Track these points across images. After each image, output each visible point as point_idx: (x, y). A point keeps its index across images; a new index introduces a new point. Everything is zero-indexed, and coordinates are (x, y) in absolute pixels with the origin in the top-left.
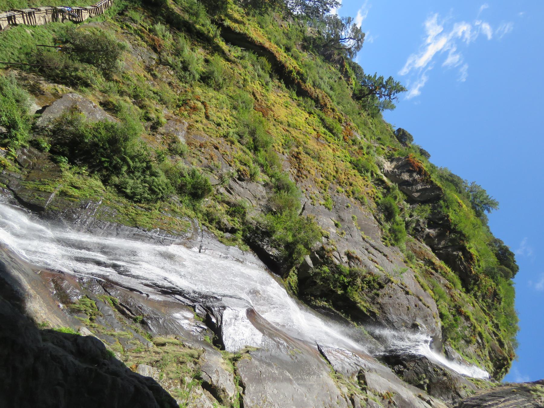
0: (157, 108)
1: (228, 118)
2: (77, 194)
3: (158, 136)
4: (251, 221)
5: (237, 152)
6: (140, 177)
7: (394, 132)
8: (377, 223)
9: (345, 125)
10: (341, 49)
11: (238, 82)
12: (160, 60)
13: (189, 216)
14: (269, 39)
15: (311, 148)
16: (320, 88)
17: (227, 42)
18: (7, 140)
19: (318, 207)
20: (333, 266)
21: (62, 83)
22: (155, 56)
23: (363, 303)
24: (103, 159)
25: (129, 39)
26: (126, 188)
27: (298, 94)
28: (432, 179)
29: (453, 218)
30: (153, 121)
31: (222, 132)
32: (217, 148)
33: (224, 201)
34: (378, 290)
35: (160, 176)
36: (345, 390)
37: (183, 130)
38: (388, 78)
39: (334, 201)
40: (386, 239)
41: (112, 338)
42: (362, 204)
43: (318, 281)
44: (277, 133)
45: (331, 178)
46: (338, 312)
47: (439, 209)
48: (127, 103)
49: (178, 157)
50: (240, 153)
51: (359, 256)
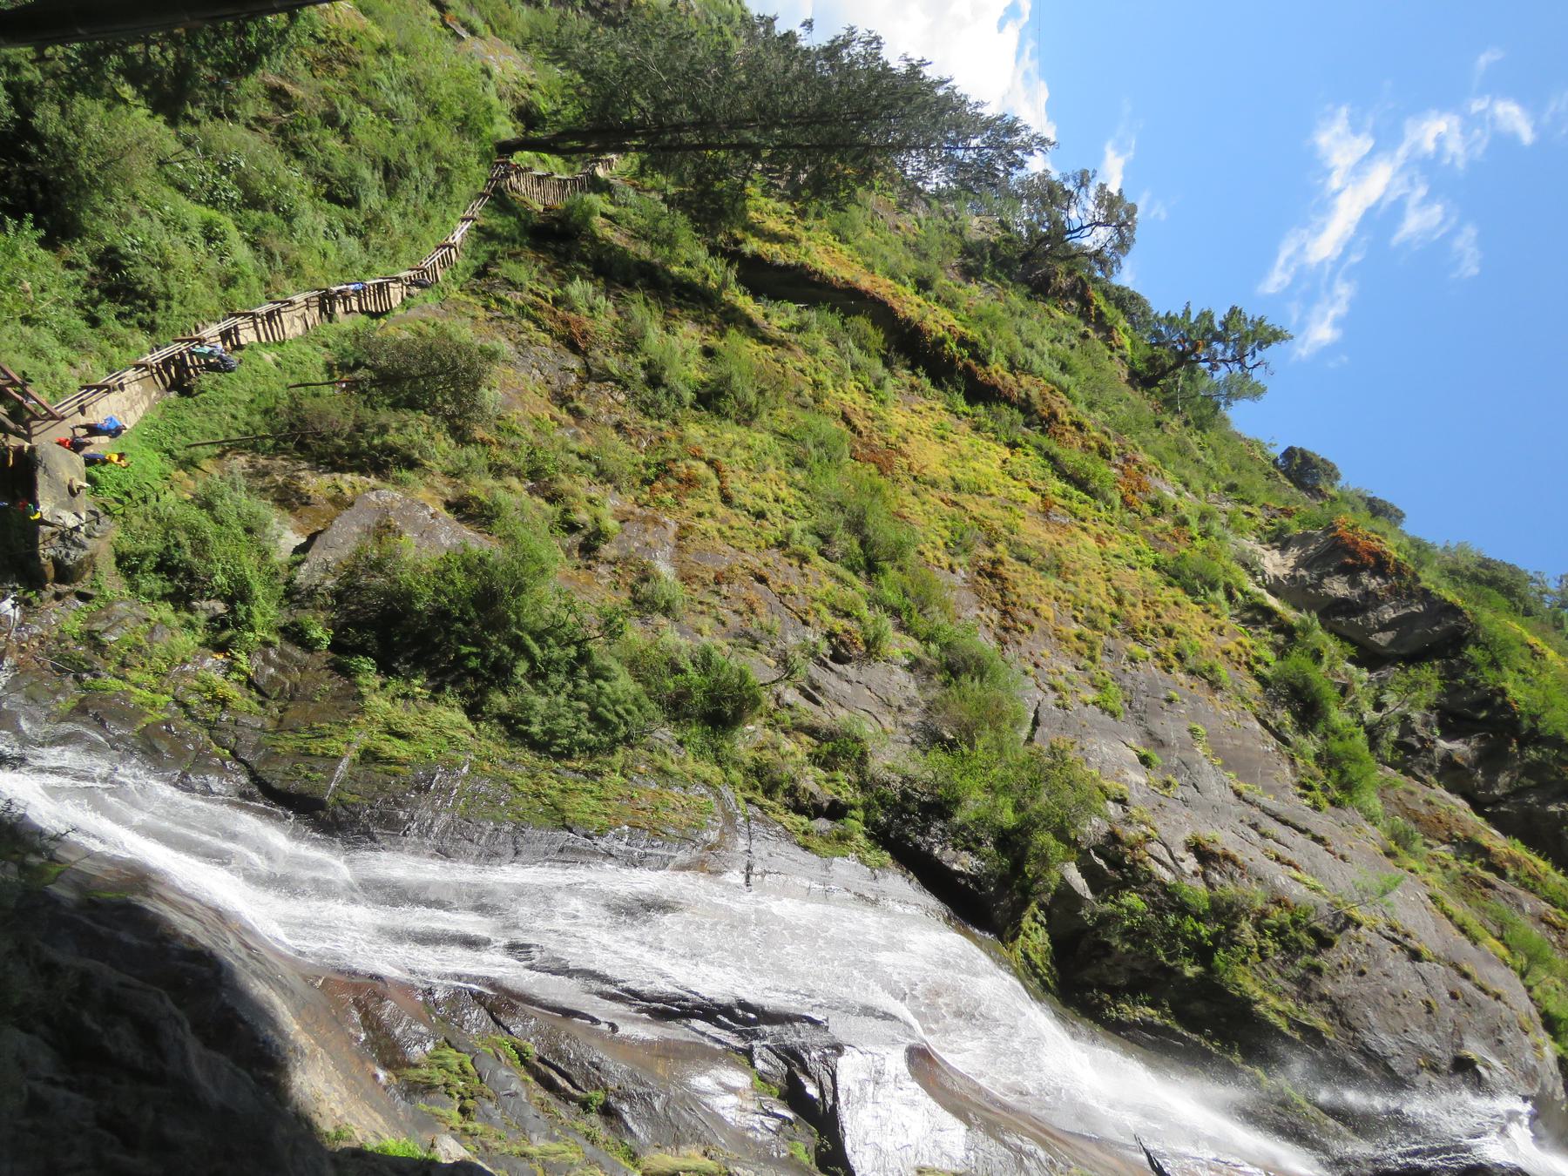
0: (593, 495)
1: (783, 494)
2: (404, 754)
3: (602, 570)
4: (884, 775)
5: (820, 583)
6: (563, 685)
7: (1275, 462)
8: (1272, 739)
9: (1120, 462)
10: (1074, 256)
11: (799, 394)
12: (588, 370)
13: (705, 782)
14: (870, 267)
15: (1032, 541)
16: (1031, 372)
17: (756, 297)
18: (228, 633)
19: (1078, 713)
20: (1156, 889)
21: (351, 470)
22: (574, 363)
23: (1272, 1001)
24: (465, 650)
25: (507, 333)
26: (528, 723)
27: (971, 399)
28: (1424, 584)
29: (1519, 696)
30: (585, 532)
31: (771, 533)
32: (762, 580)
33: (799, 728)
34: (1315, 954)
35: (616, 679)
37: (664, 543)
38: (1226, 311)
39: (1124, 688)
40: (1310, 788)
41: (526, 1165)
42: (1215, 686)
43: (1115, 942)
44: (926, 513)
45: (1106, 621)
46: (1195, 1037)
47: (1471, 675)
48: (514, 496)
49: (659, 619)
50: (830, 584)
51: (1232, 851)
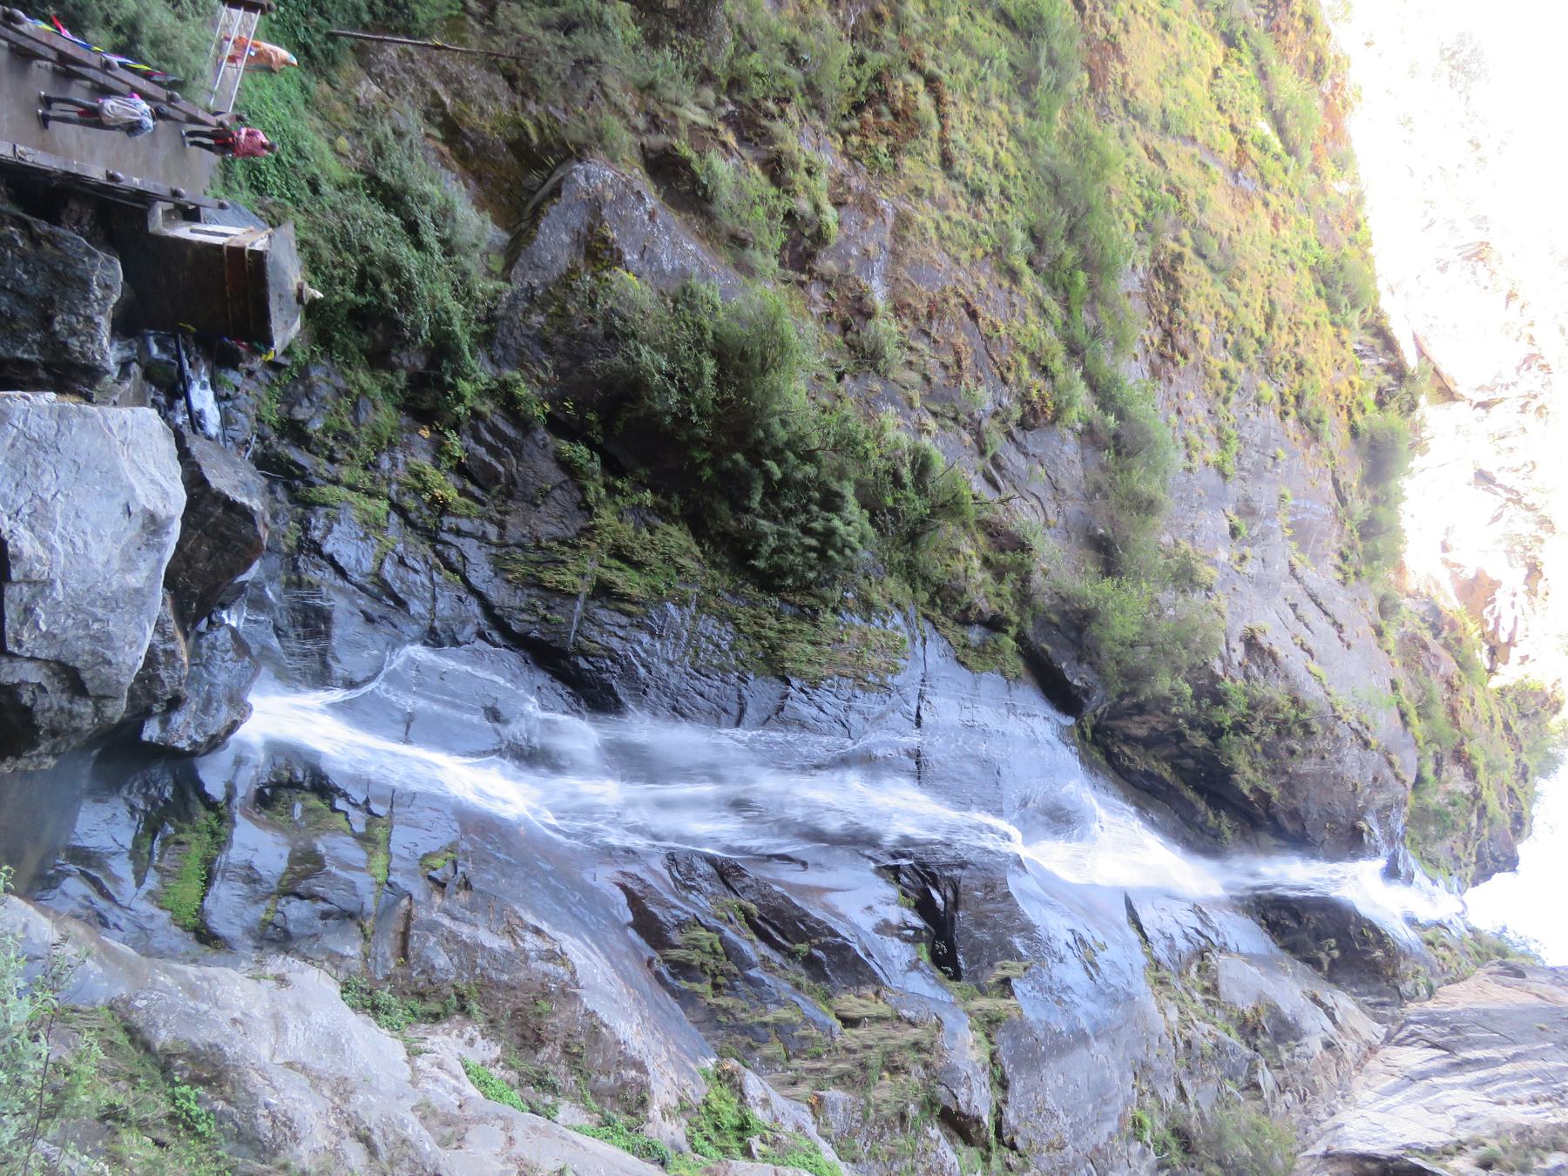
3: (815, 291)
8: (1334, 501)
23: (1250, 774)
32: (973, 315)
36: (1174, 1015)
45: (1250, 346)
51: (1276, 648)
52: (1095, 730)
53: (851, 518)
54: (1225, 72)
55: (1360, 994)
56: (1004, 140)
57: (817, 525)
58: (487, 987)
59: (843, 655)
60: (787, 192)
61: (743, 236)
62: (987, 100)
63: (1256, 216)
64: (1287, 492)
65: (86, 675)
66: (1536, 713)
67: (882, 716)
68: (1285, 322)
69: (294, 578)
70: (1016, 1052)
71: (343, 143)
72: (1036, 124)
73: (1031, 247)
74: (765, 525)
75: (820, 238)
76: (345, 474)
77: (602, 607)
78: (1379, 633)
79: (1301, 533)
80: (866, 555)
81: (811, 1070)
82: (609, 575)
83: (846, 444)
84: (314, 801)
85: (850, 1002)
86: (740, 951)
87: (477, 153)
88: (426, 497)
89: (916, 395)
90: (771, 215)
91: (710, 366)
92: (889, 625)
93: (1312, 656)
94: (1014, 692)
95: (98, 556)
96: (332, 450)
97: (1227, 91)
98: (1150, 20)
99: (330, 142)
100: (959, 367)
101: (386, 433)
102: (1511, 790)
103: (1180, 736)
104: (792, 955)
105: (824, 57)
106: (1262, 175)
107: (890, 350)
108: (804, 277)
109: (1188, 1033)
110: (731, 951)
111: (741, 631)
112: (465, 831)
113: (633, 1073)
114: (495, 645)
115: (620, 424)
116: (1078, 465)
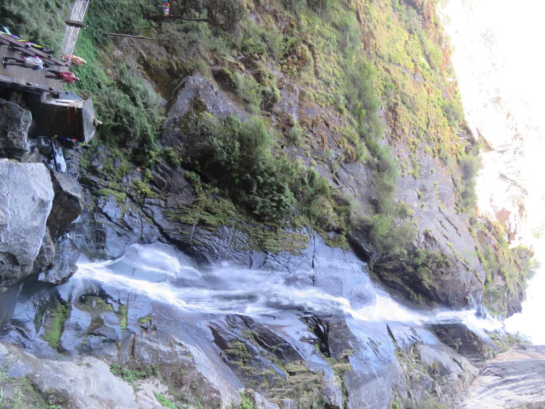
3: (273, 118)
8: (453, 186)
23: (428, 281)
32: (327, 125)
36: (405, 367)
45: (422, 134)
51: (435, 237)
52: (374, 267)
53: (288, 195)
54: (409, 42)
55: (470, 358)
56: (336, 66)
57: (276, 198)
58: (162, 365)
59: (286, 243)
60: (262, 84)
61: (248, 99)
62: (330, 53)
63: (422, 90)
64: (437, 183)
65: (18, 258)
66: (525, 257)
67: (300, 264)
68: (433, 125)
69: (93, 221)
70: (351, 383)
71: (109, 71)
72: (346, 60)
73: (346, 101)
74: (258, 198)
75: (274, 100)
76: (111, 184)
77: (202, 228)
78: (470, 230)
79: (442, 196)
80: (293, 208)
81: (278, 392)
82: (204, 217)
83: (285, 170)
84: (100, 300)
85: (292, 366)
86: (252, 349)
87: (156, 72)
88: (139, 192)
89: (309, 152)
90: (257, 92)
91: (237, 144)
92: (302, 232)
93: (448, 239)
94: (346, 254)
95: (23, 215)
96: (106, 176)
97: (411, 49)
98: (383, 25)
99: (105, 70)
100: (323, 143)
101: (125, 170)
102: (518, 284)
103: (404, 268)
104: (271, 350)
105: (274, 39)
106: (423, 76)
107: (299, 138)
108: (269, 113)
109: (411, 373)
110: (249, 350)
111: (250, 236)
112: (154, 309)
113: (215, 395)
114: (163, 242)
115: (207, 165)
116: (365, 175)
